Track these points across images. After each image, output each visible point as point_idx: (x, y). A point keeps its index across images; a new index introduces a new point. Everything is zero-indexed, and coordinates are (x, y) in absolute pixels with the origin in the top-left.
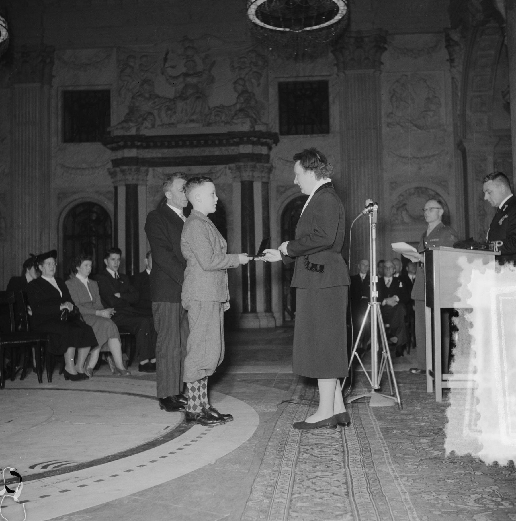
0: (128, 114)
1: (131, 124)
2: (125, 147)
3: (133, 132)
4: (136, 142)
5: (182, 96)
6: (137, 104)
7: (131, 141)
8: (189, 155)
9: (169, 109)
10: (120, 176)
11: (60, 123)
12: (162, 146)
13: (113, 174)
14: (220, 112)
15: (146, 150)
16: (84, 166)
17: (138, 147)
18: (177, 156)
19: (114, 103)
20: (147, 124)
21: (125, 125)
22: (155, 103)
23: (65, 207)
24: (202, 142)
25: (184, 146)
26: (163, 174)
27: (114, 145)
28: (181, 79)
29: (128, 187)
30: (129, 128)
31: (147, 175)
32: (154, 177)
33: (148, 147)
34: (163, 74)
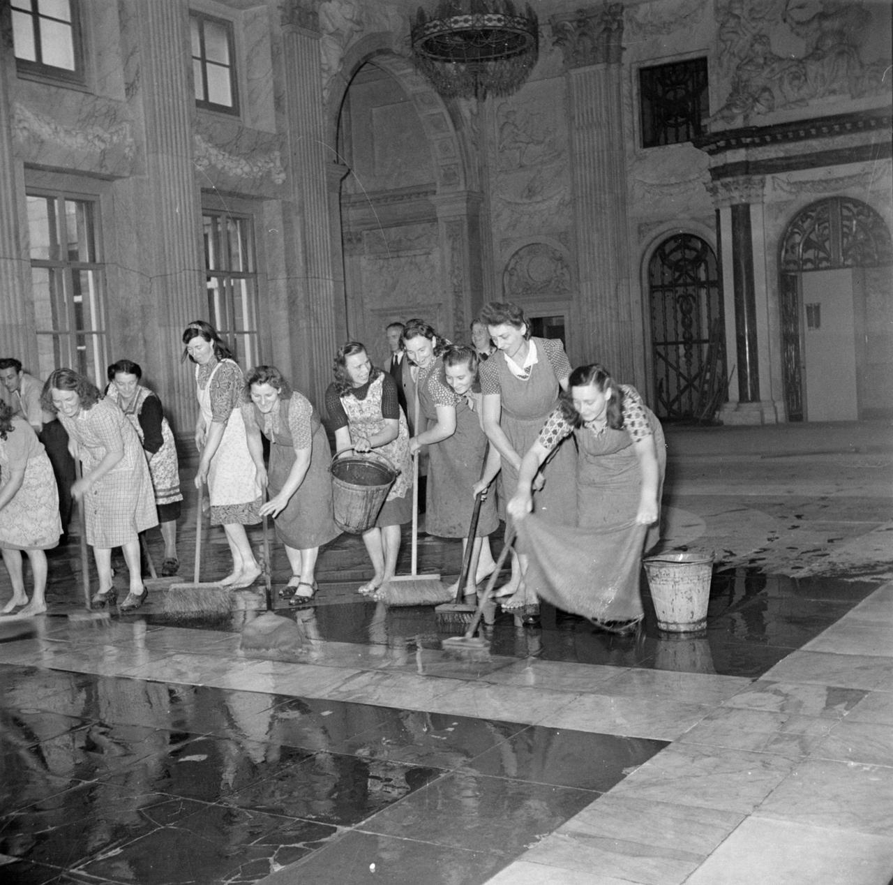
0: (731, 95)
1: (735, 111)
2: (728, 147)
3: (738, 123)
4: (743, 139)
5: (816, 54)
6: (745, 77)
7: (734, 139)
8: (827, 149)
9: (796, 77)
10: (722, 191)
11: (636, 118)
12: (786, 139)
13: (713, 191)
14: (877, 71)
15: (760, 149)
16: (673, 180)
17: (747, 146)
18: (809, 152)
19: (712, 78)
20: (760, 107)
21: (726, 113)
22: (773, 70)
23: (656, 238)
24: (848, 126)
25: (819, 135)
26: (789, 183)
27: (713, 147)
28: (815, 25)
29: (734, 209)
30: (733, 118)
31: (763, 187)
32: (775, 189)
33: (763, 143)
34: (785, 21)
